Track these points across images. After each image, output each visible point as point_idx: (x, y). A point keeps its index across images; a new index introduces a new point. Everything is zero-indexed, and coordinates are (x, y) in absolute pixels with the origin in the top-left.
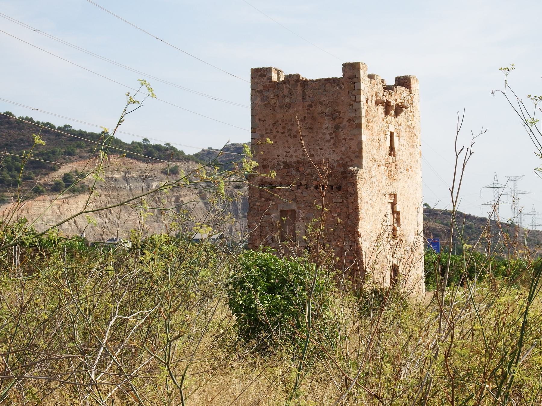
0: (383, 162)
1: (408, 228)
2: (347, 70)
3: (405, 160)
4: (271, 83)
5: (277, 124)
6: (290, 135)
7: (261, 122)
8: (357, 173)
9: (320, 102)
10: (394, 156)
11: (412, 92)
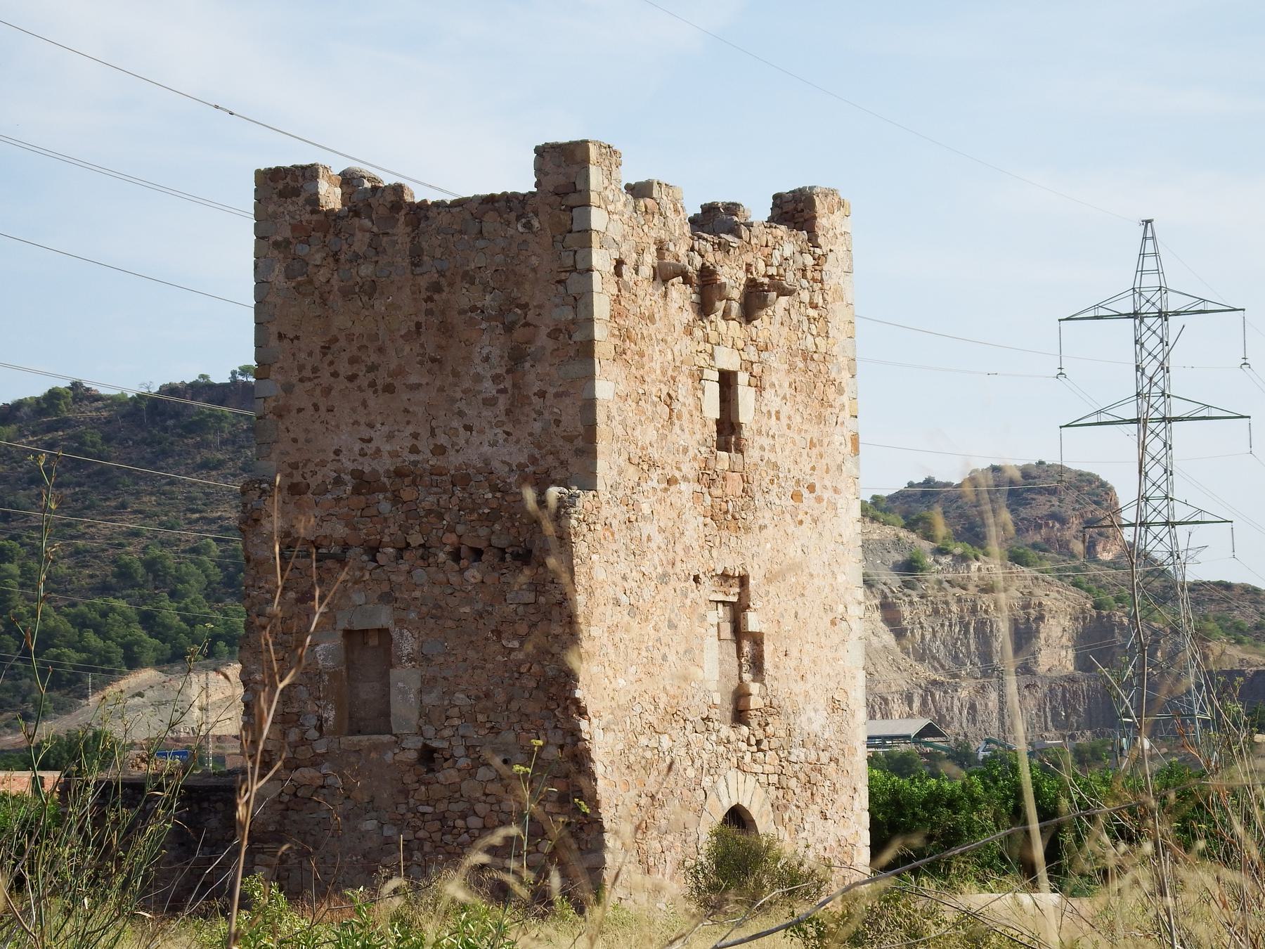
1: (799, 688)
2: (549, 167)
4: (315, 217)
5: (335, 347)
6: (372, 384)
7: (286, 342)
8: (573, 505)
9: (466, 274)
10: (740, 450)
11: (821, 240)
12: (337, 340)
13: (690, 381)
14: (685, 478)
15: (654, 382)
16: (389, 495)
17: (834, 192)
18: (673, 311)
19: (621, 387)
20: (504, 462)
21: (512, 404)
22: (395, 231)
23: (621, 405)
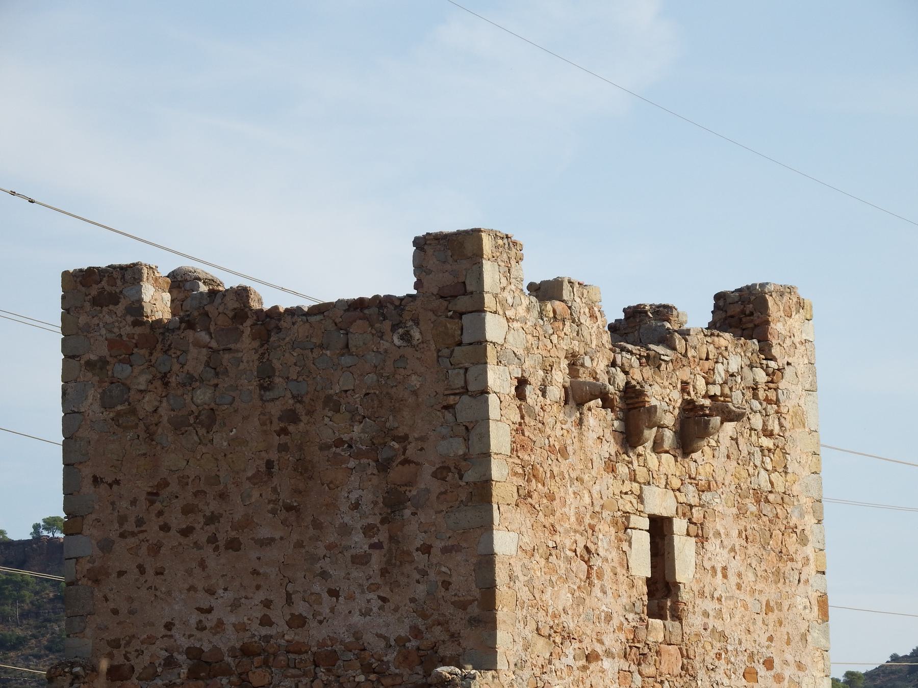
0: (613, 641)
3: (735, 632)
4: (138, 330)
5: (165, 493)
6: (213, 539)
7: (103, 488)
9: (328, 398)
11: (776, 351)
12: (167, 484)
13: (613, 530)
14: (609, 654)
15: (567, 532)
16: (234, 679)
17: (791, 290)
18: (590, 442)
19: (526, 539)
20: (379, 636)
21: (389, 562)
22: (239, 346)
23: (526, 561)
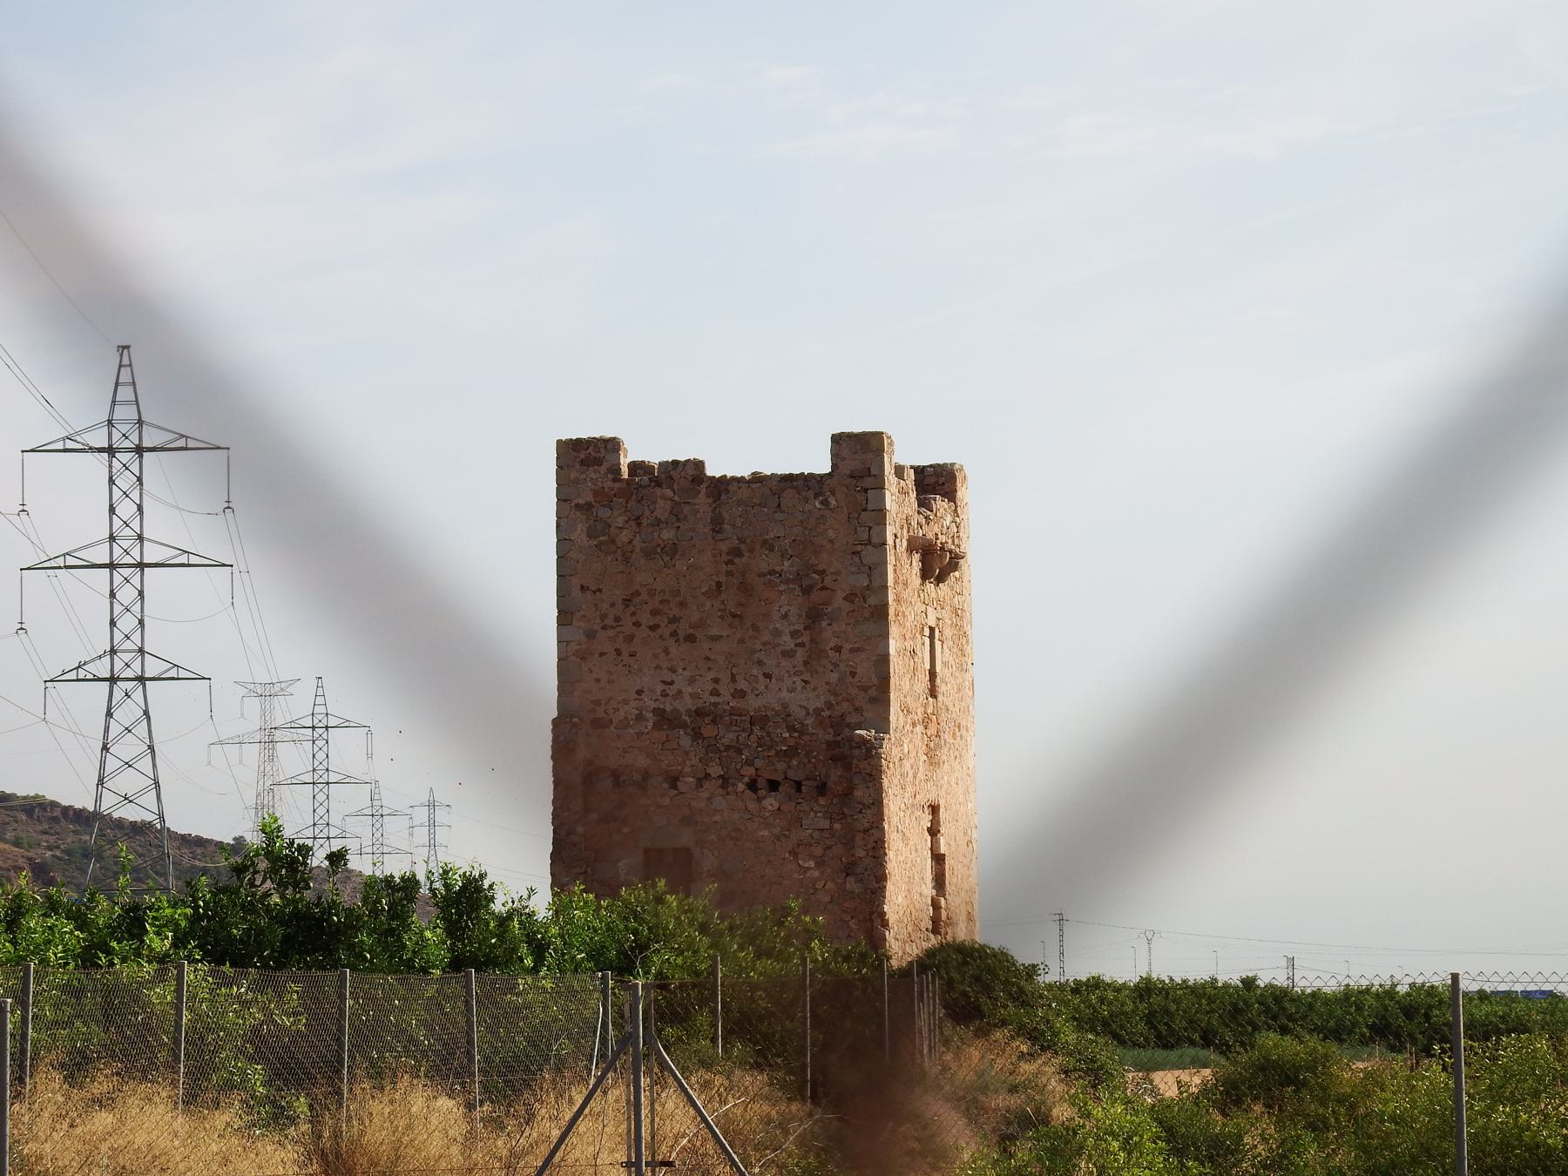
2: (845, 452)
4: (617, 485)
5: (636, 600)
6: (674, 634)
9: (765, 542)
